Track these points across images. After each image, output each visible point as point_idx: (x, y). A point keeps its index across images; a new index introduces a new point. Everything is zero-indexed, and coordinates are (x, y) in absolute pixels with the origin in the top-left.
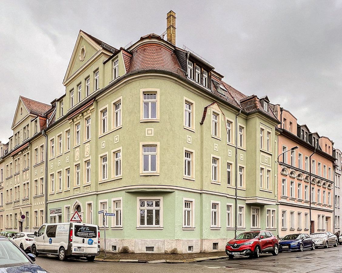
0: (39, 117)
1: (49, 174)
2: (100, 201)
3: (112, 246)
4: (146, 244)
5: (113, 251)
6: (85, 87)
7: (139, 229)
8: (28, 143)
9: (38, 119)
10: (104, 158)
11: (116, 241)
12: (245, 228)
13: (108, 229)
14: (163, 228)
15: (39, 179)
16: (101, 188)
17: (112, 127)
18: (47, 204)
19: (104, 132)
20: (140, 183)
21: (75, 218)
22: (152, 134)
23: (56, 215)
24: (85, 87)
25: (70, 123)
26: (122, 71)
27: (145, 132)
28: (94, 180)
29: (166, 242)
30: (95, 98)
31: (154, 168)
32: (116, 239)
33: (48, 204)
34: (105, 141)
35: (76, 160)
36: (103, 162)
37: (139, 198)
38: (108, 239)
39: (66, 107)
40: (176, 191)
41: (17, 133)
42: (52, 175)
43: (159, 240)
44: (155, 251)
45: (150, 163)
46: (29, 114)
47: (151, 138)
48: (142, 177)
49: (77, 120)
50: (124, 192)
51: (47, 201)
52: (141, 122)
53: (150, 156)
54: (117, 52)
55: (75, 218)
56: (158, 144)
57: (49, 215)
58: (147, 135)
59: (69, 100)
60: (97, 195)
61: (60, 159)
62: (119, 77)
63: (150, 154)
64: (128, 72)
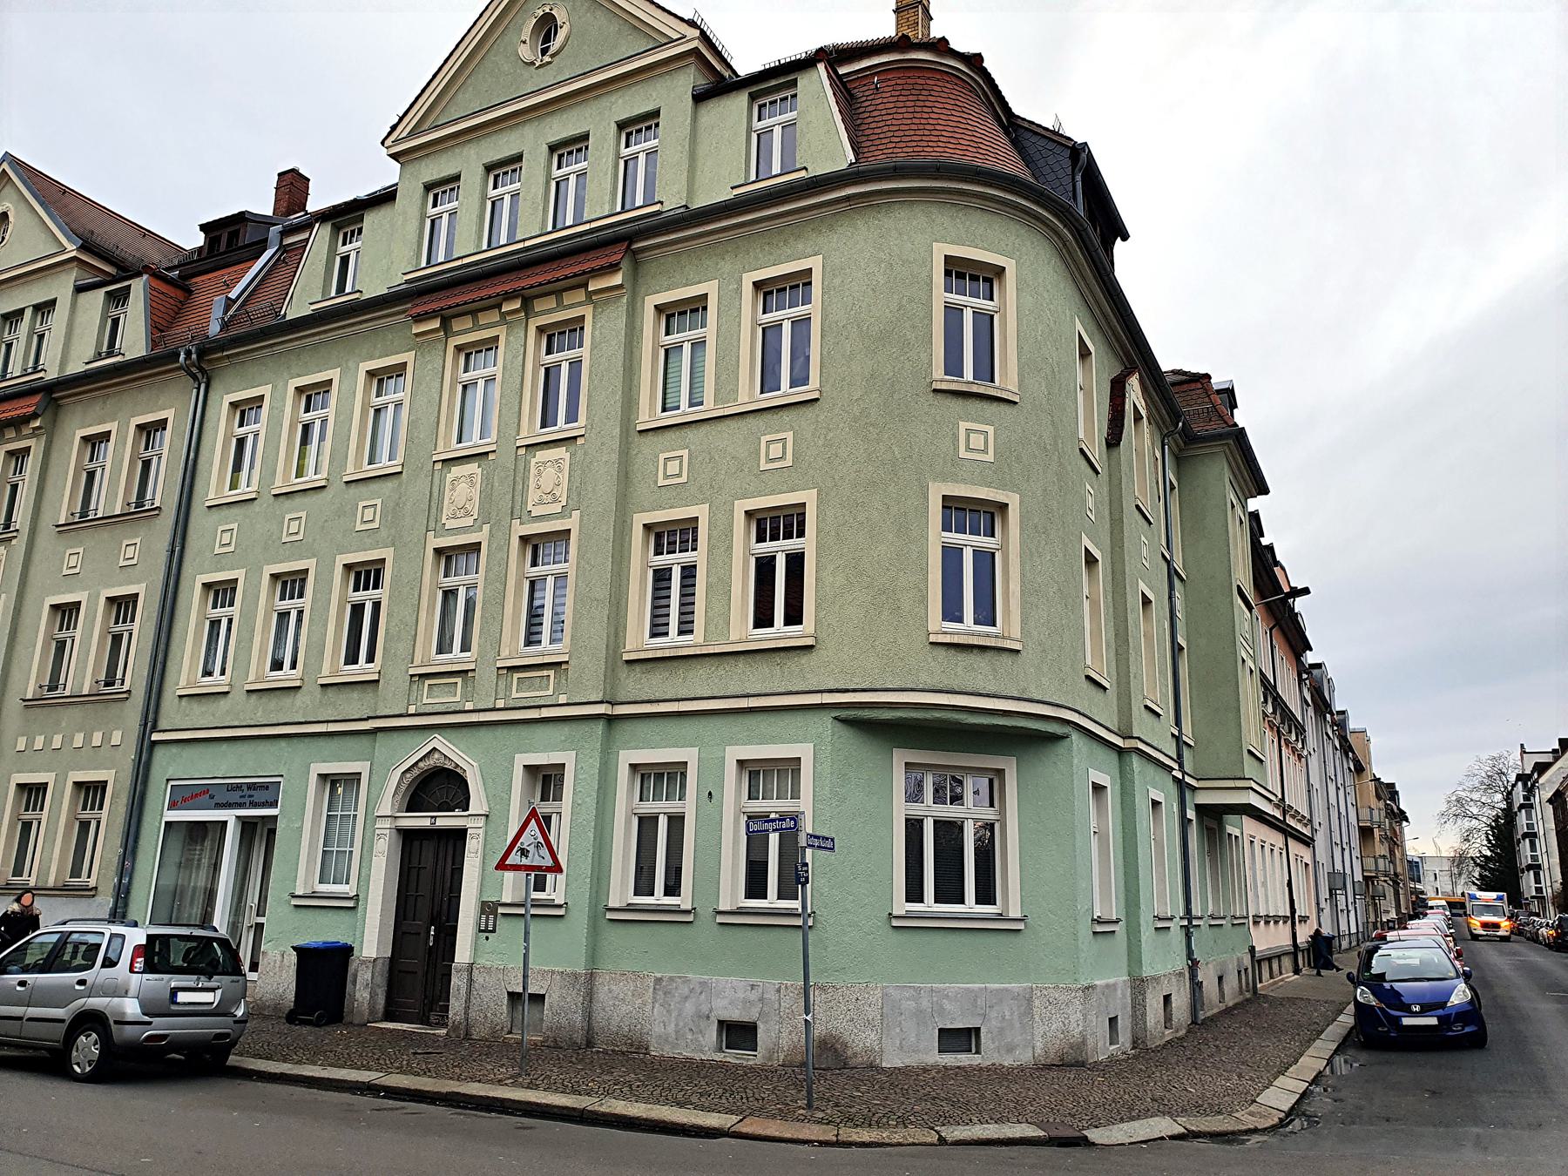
0: (145, 277)
1: (195, 580)
2: (628, 756)
3: (721, 1023)
4: (942, 1011)
5: (721, 1050)
6: (548, 183)
7: (902, 928)
8: (38, 398)
9: (138, 286)
10: (66, 612)
11: (754, 996)
12: (1019, 916)
13: (690, 918)
14: (1021, 926)
15: (93, 598)
16: (635, 685)
17: (441, 443)
18: (147, 750)
19: (233, 486)
20: (925, 679)
21: (524, 853)
22: (985, 451)
23: (229, 816)
24: (548, 183)
25: (417, 335)
26: (134, 342)
27: (956, 437)
28: (597, 636)
29: (1037, 1003)
30: (630, 238)
31: (986, 615)
32: (753, 980)
33: (159, 753)
34: (138, 541)
35: (450, 524)
36: (214, 607)
37: (900, 757)
38: (687, 981)
39: (383, 260)
40: (1075, 736)
41: (21, 312)
42: (222, 592)
43: (1007, 990)
44: (990, 1054)
45: (972, 587)
46: (73, 254)
47: (983, 473)
48: (942, 652)
49: (19, 438)
50: (826, 719)
51: (154, 729)
52: (934, 386)
53: (968, 556)
54: (127, 270)
55: (524, 853)
56: (1013, 500)
57: (162, 814)
58: (962, 453)
59: (415, 223)
60: (610, 720)
61: (298, 511)
62: (803, 174)
63: (970, 542)
64: (154, 343)
